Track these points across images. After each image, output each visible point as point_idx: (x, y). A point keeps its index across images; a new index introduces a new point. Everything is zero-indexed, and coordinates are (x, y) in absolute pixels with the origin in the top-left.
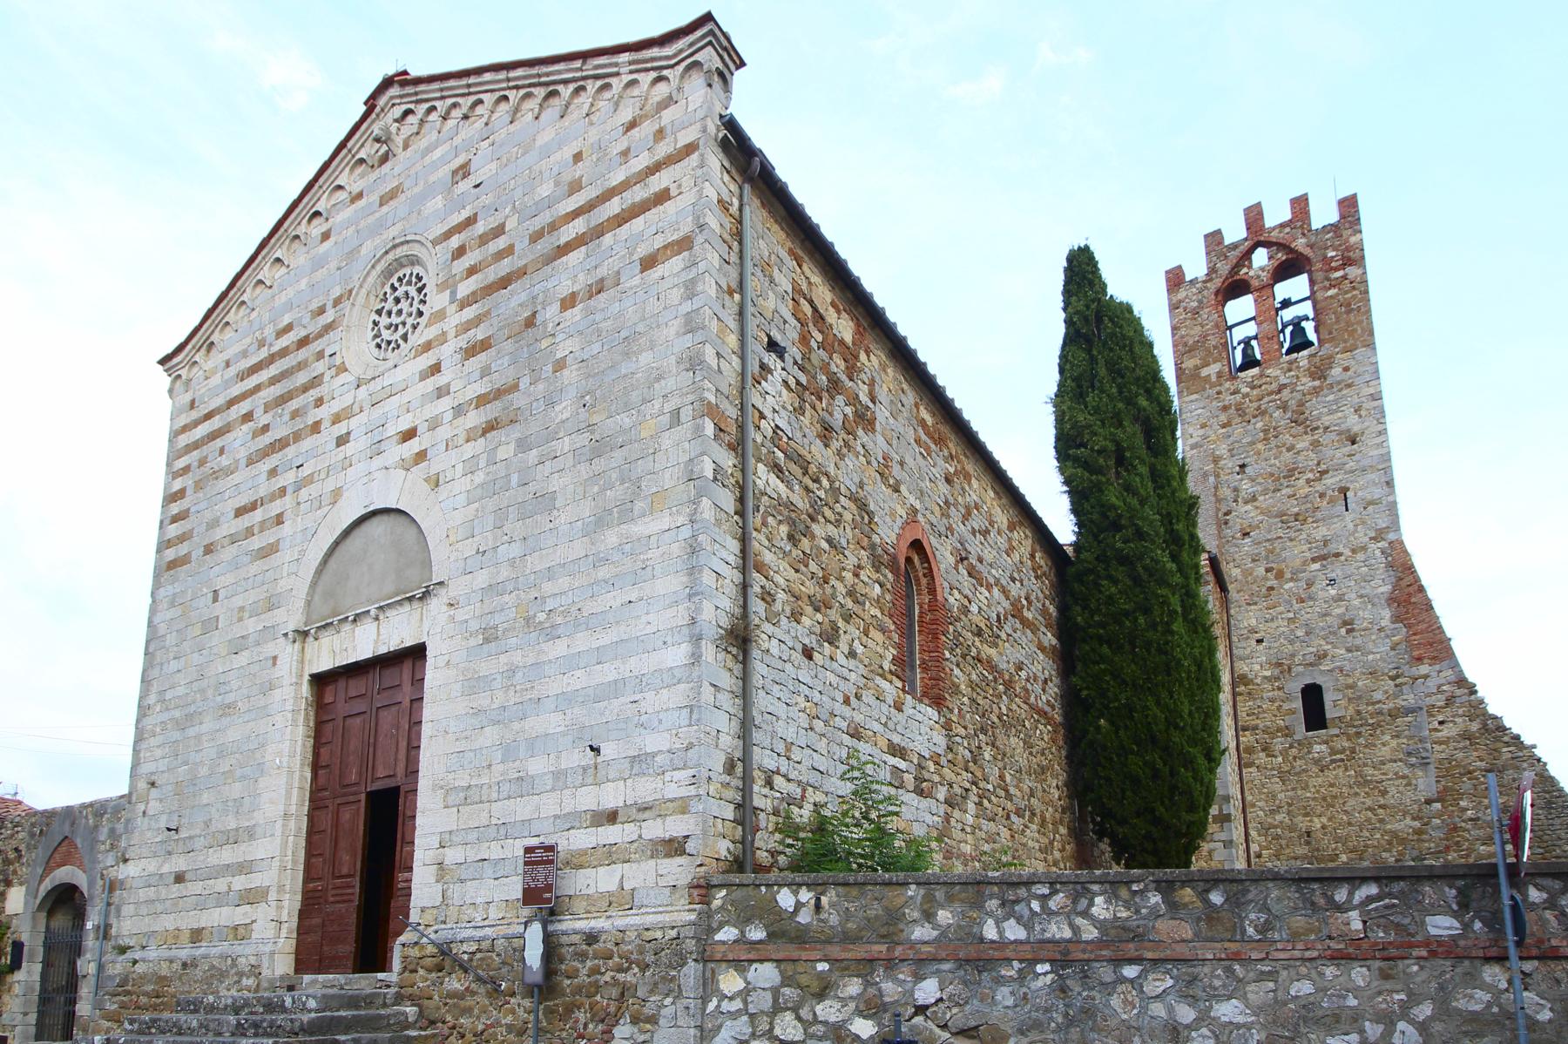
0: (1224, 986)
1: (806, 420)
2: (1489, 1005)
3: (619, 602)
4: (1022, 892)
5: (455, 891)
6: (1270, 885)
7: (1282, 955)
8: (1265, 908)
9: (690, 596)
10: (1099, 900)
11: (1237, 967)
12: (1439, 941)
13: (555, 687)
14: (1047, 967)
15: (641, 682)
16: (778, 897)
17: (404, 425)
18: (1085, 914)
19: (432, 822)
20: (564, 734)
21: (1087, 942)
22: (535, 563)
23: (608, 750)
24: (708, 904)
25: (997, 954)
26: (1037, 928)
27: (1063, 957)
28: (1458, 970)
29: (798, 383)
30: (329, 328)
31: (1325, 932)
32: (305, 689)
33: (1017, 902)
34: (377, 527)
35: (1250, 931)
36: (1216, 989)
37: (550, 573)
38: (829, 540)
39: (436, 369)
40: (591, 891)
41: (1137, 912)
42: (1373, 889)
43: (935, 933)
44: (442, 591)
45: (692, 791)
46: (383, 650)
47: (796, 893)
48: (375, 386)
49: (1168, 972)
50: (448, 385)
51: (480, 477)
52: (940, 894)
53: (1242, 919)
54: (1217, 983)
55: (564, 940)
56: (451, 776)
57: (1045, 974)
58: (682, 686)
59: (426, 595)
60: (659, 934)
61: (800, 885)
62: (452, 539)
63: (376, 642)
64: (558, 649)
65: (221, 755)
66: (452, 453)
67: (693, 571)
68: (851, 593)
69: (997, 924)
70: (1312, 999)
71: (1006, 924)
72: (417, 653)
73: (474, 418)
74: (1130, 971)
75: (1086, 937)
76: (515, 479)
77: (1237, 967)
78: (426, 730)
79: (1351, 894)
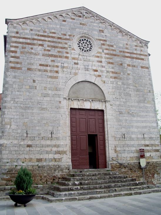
13: (135, 124)
23: (145, 136)
44: (109, 102)
64: (135, 119)
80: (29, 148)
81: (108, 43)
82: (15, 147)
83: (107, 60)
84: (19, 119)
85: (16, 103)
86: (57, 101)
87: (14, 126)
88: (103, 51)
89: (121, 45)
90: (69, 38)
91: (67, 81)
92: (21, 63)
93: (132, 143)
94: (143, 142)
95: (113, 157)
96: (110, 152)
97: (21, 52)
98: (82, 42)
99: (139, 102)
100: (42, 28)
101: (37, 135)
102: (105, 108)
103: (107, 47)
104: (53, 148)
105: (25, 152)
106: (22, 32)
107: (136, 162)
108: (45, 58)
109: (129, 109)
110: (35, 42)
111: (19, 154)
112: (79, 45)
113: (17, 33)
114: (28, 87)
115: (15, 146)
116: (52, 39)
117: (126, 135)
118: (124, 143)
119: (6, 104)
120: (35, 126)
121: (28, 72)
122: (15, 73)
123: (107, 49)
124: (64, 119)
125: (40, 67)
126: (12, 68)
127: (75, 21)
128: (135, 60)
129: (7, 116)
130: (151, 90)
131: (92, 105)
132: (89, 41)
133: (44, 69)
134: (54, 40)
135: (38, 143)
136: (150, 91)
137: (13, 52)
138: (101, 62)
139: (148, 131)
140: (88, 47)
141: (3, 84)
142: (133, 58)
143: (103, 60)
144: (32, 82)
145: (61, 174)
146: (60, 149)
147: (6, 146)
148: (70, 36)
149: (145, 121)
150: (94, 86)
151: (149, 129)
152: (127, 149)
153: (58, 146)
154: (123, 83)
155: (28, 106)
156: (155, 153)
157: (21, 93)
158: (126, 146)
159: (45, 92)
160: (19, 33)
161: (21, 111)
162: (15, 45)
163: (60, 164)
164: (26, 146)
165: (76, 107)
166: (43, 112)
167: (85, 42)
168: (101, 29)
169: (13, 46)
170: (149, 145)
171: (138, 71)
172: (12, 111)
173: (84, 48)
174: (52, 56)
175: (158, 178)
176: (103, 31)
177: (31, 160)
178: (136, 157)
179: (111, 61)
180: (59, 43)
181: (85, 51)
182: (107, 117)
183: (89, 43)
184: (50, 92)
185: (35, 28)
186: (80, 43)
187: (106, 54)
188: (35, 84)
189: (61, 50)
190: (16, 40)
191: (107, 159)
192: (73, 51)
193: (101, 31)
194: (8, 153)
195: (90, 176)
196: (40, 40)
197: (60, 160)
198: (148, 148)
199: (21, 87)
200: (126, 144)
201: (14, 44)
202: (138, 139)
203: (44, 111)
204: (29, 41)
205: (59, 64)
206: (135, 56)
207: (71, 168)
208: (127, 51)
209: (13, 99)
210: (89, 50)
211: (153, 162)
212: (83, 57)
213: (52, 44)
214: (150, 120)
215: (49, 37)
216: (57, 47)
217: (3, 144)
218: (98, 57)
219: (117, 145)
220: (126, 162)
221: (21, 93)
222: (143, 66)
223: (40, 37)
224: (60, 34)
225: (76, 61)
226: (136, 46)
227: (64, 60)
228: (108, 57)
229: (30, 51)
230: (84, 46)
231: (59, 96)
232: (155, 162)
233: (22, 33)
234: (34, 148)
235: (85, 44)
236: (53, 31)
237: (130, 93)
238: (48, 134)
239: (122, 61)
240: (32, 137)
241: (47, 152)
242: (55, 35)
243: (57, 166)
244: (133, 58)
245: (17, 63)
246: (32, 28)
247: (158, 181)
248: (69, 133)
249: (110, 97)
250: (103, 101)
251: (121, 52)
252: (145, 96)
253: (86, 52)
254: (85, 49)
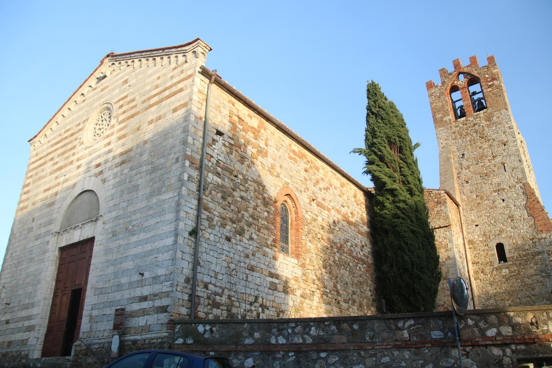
0: (357, 360)
1: (232, 157)
2: (454, 364)
3: (154, 222)
4: (285, 326)
5: (94, 325)
6: (375, 321)
7: (378, 347)
8: (373, 330)
9: (176, 220)
10: (313, 328)
11: (362, 352)
12: (436, 340)
13: (132, 252)
14: (293, 354)
15: (158, 251)
16: (198, 328)
17: (98, 162)
18: (308, 334)
19: (90, 299)
20: (133, 269)
21: (308, 344)
22: (131, 209)
23: (147, 275)
24: (174, 330)
25: (275, 349)
26: (290, 339)
27: (299, 350)
28: (442, 351)
29: (230, 144)
30: (80, 130)
31: (395, 338)
32: (57, 253)
33: (283, 330)
34: (86, 196)
35: (368, 338)
36: (354, 361)
37: (135, 212)
38: (242, 197)
39: (109, 144)
40: (137, 326)
41: (327, 333)
42: (412, 322)
43: (253, 341)
45: (171, 289)
46: (82, 239)
47: (204, 326)
48: (91, 149)
49: (337, 355)
50: (112, 149)
51: (117, 179)
52: (255, 327)
53: (365, 334)
54: (355, 358)
55: (126, 343)
56: (97, 284)
57: (292, 356)
58: (171, 252)
59: (97, 220)
60: (155, 341)
61: (206, 323)
62: (107, 200)
63: (80, 236)
64: (134, 239)
65: (27, 277)
66: (110, 171)
67: (178, 212)
68: (252, 216)
69: (276, 338)
70: (389, 364)
71: (279, 338)
72: (91, 241)
73: (118, 160)
74: (323, 355)
75: (308, 342)
76: (128, 180)
77: (362, 352)
78: (92, 267)
79: (404, 324)
94: (139, 292)
99: (152, 195)
151: (157, 256)
156: (156, 315)
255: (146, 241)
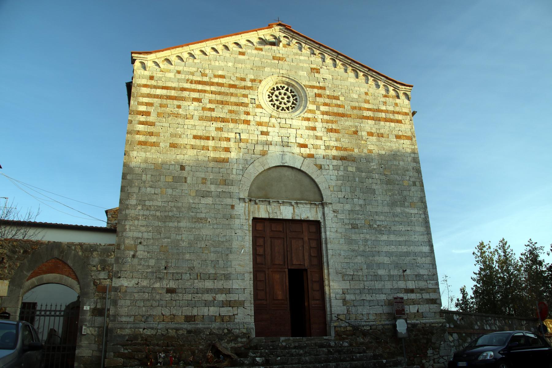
13: (385, 249)
23: (408, 272)
44: (330, 206)
58: (429, 258)
64: (385, 238)
80: (170, 294)
81: (328, 92)
82: (144, 292)
83: (325, 125)
84: (153, 239)
85: (147, 209)
86: (227, 205)
87: (142, 252)
88: (318, 108)
89: (355, 96)
90: (251, 85)
91: (247, 166)
92: (158, 135)
93: (378, 285)
94: (402, 284)
95: (339, 312)
96: (332, 304)
97: (159, 115)
98: (277, 93)
99: (393, 204)
100: (198, 68)
101: (187, 269)
102: (322, 217)
103: (327, 101)
104: (217, 296)
105: (161, 302)
106: (161, 76)
107: (388, 325)
108: (205, 124)
109: (371, 218)
110: (186, 94)
111: (152, 306)
112: (271, 99)
113: (152, 78)
114: (170, 179)
115: (142, 290)
116: (217, 87)
117: (366, 271)
118: (362, 286)
119: (128, 212)
120: (184, 254)
121: (171, 150)
122: (145, 152)
123: (325, 104)
124: (240, 239)
125: (193, 142)
126: (141, 143)
127: (263, 53)
128: (382, 123)
129: (130, 234)
130: (418, 180)
131: (296, 211)
132: (291, 90)
133: (203, 144)
134: (223, 89)
135: (188, 284)
136: (414, 184)
137: (142, 113)
138: (314, 129)
139: (413, 261)
140: (288, 102)
141: (121, 174)
142: (379, 119)
143: (319, 125)
144: (179, 169)
145: (233, 345)
146: (233, 297)
147: (126, 291)
148: (253, 81)
149: (406, 243)
150: (300, 176)
152: (368, 298)
153: (229, 291)
154: (358, 169)
155: (170, 214)
156: (427, 305)
157: (158, 191)
158: (366, 291)
159: (203, 188)
160: (155, 78)
161: (156, 225)
162: (147, 101)
163: (231, 326)
164: (165, 291)
165: (263, 215)
166: (199, 226)
167: (283, 91)
168: (314, 66)
169: (142, 102)
170: (415, 290)
171: (389, 144)
172: (139, 224)
173: (280, 103)
174: (216, 119)
175: (436, 357)
176: (318, 71)
177: (173, 317)
178: (388, 313)
179: (334, 127)
180: (232, 94)
181: (283, 109)
182: (326, 235)
183: (290, 94)
184: (213, 188)
185: (186, 69)
186: (272, 94)
187: (323, 113)
188: (184, 174)
189: (235, 108)
190: (148, 92)
191: (328, 319)
192: (259, 110)
193: (315, 71)
194: (129, 305)
195: (289, 348)
196: (194, 90)
197: (231, 318)
198: (413, 296)
199: (158, 179)
200: (366, 288)
201: (146, 100)
202: (391, 277)
203: (201, 224)
204: (173, 93)
205: (232, 135)
206: (383, 115)
207: (253, 335)
208: (367, 106)
209: (141, 202)
210: (290, 108)
211: (425, 324)
212: (279, 120)
213: (219, 98)
214: (415, 240)
215: (212, 84)
216: (227, 103)
217: (120, 286)
218: (308, 119)
219: (347, 289)
220: (367, 323)
221: (158, 191)
222: (400, 133)
223: (194, 85)
224: (234, 79)
225: (264, 129)
226: (385, 96)
227: (242, 126)
228: (328, 119)
229: (176, 111)
230: (281, 100)
231: (230, 195)
232: (428, 325)
233: (160, 79)
234: (180, 295)
235: (283, 96)
236: (220, 73)
237: (374, 187)
238: (209, 268)
239: (356, 127)
240: (177, 273)
241: (207, 304)
242: (225, 80)
243: (226, 331)
244: (379, 119)
245: (151, 134)
246: (180, 68)
247: (434, 363)
248: (249, 266)
249: (333, 196)
250: (317, 203)
251: (354, 108)
252: (405, 193)
253: (285, 110)
254: (283, 105)
255: (400, 243)
